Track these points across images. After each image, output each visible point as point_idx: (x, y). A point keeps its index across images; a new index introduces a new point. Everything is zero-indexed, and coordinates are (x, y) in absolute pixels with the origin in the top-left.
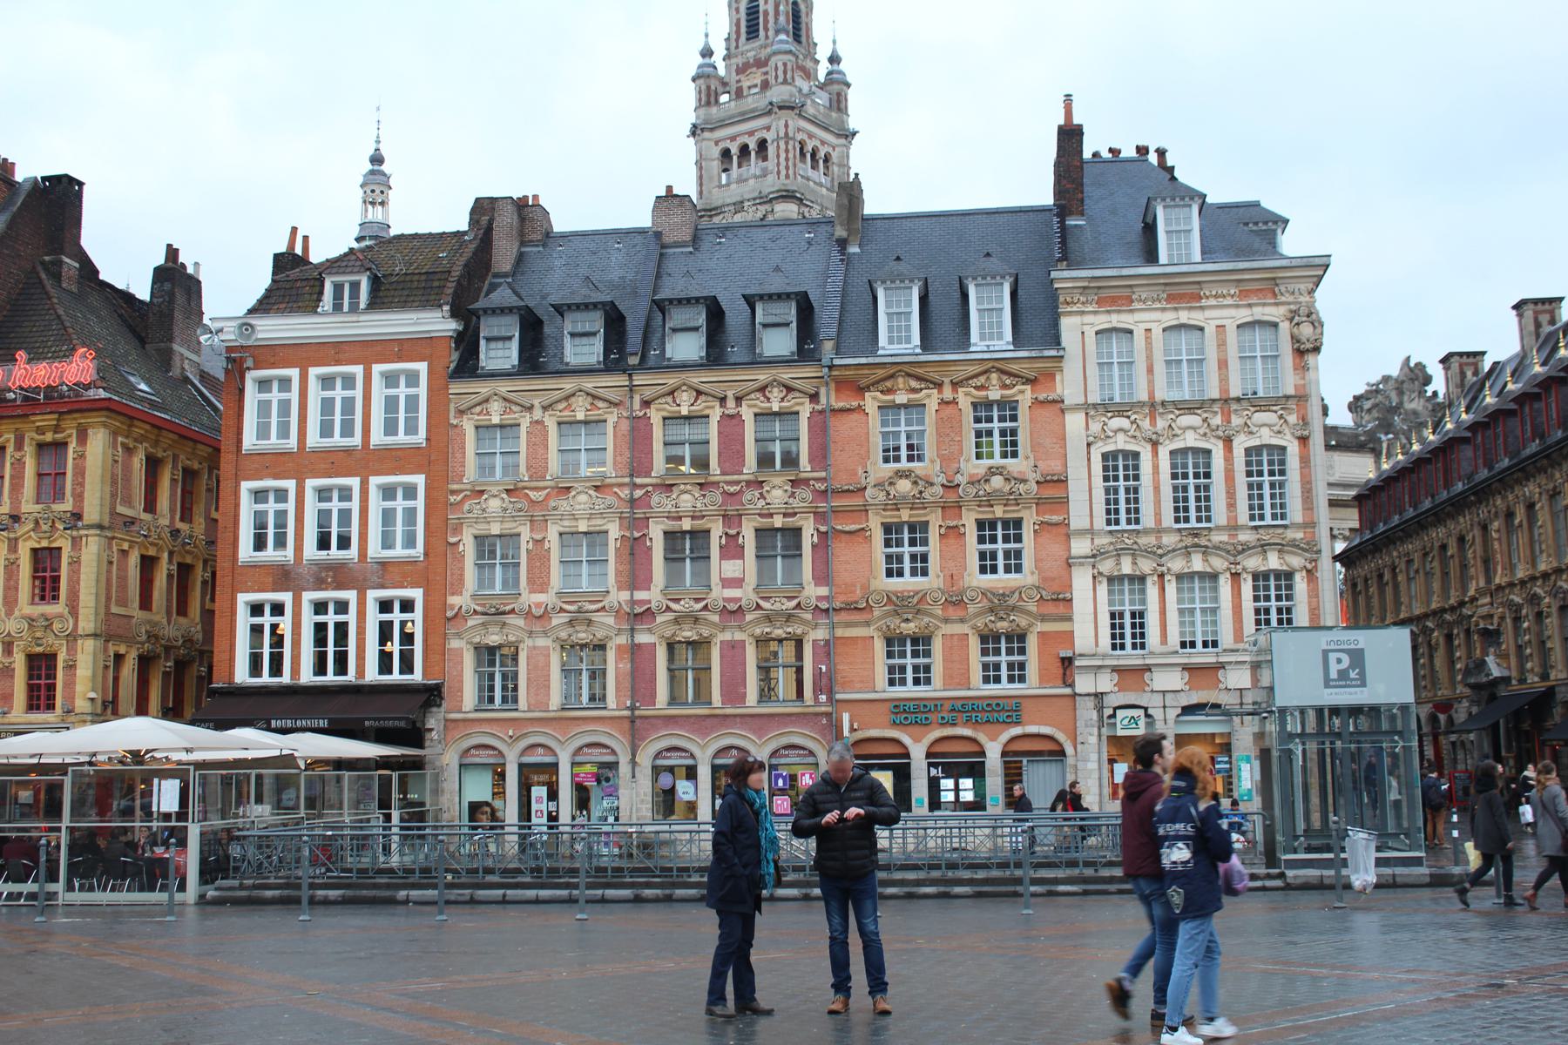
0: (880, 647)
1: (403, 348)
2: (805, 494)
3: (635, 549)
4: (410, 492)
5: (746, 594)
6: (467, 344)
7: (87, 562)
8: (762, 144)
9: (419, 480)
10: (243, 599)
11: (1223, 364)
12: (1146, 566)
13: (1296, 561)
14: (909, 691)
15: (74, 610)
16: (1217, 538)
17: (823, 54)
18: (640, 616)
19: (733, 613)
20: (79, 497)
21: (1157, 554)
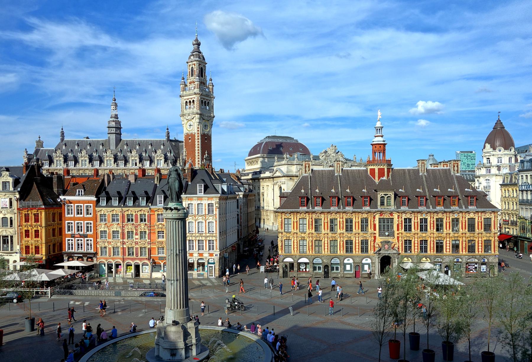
0: (157, 249)
1: (89, 202)
2: (146, 226)
3: (123, 234)
4: (91, 224)
5: (139, 240)
6: (98, 201)
7: (43, 233)
8: (193, 101)
9: (92, 222)
10: (67, 239)
11: (205, 209)
12: (194, 238)
13: (214, 238)
14: (160, 255)
15: (41, 239)
16: (204, 235)
17: (208, 79)
18: (123, 243)
19: (136, 243)
20: (41, 222)
21: (196, 237)
